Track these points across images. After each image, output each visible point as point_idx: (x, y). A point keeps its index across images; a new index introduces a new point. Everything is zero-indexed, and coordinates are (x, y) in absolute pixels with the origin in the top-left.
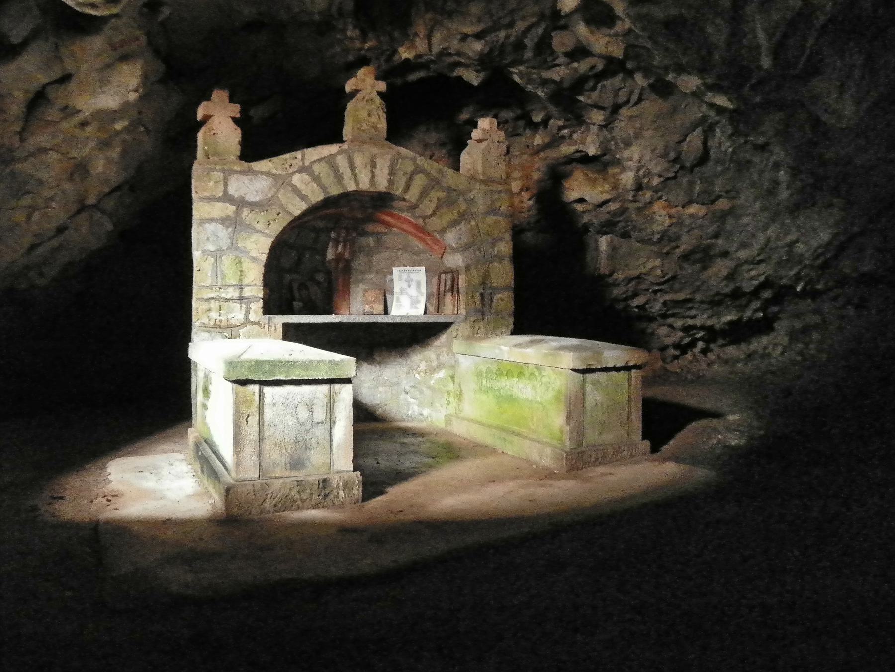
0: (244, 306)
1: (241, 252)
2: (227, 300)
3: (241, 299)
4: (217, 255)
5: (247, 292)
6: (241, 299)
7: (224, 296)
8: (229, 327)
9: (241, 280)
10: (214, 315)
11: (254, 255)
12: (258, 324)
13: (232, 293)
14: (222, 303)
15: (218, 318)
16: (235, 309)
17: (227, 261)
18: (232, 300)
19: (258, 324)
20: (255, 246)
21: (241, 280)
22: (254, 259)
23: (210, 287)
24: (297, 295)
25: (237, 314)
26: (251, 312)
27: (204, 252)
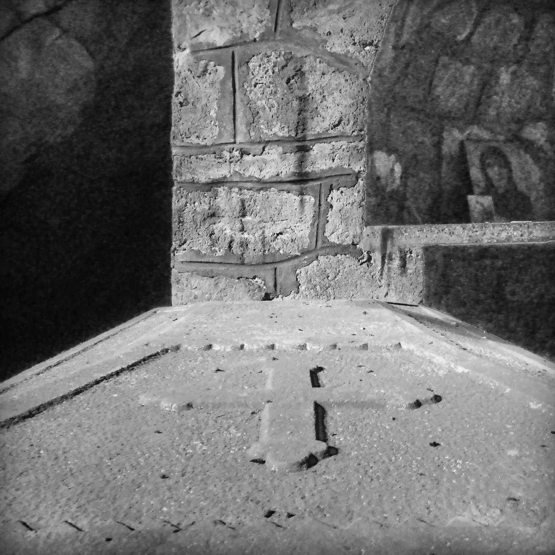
0: (310, 199)
1: (304, 43)
2: (263, 185)
3: (301, 179)
4: (234, 57)
5: (321, 159)
6: (301, 179)
7: (253, 172)
8: (270, 261)
9: (302, 124)
10: (226, 227)
11: (338, 49)
12: (351, 249)
13: (277, 163)
14: (247, 194)
15: (238, 237)
16: (286, 211)
17: (261, 70)
18: (277, 182)
19: (351, 249)
20: (342, 24)
21: (302, 124)
22: (340, 63)
23: (215, 150)
24: (475, 173)
25: (289, 220)
26: (333, 217)
27: (196, 50)
